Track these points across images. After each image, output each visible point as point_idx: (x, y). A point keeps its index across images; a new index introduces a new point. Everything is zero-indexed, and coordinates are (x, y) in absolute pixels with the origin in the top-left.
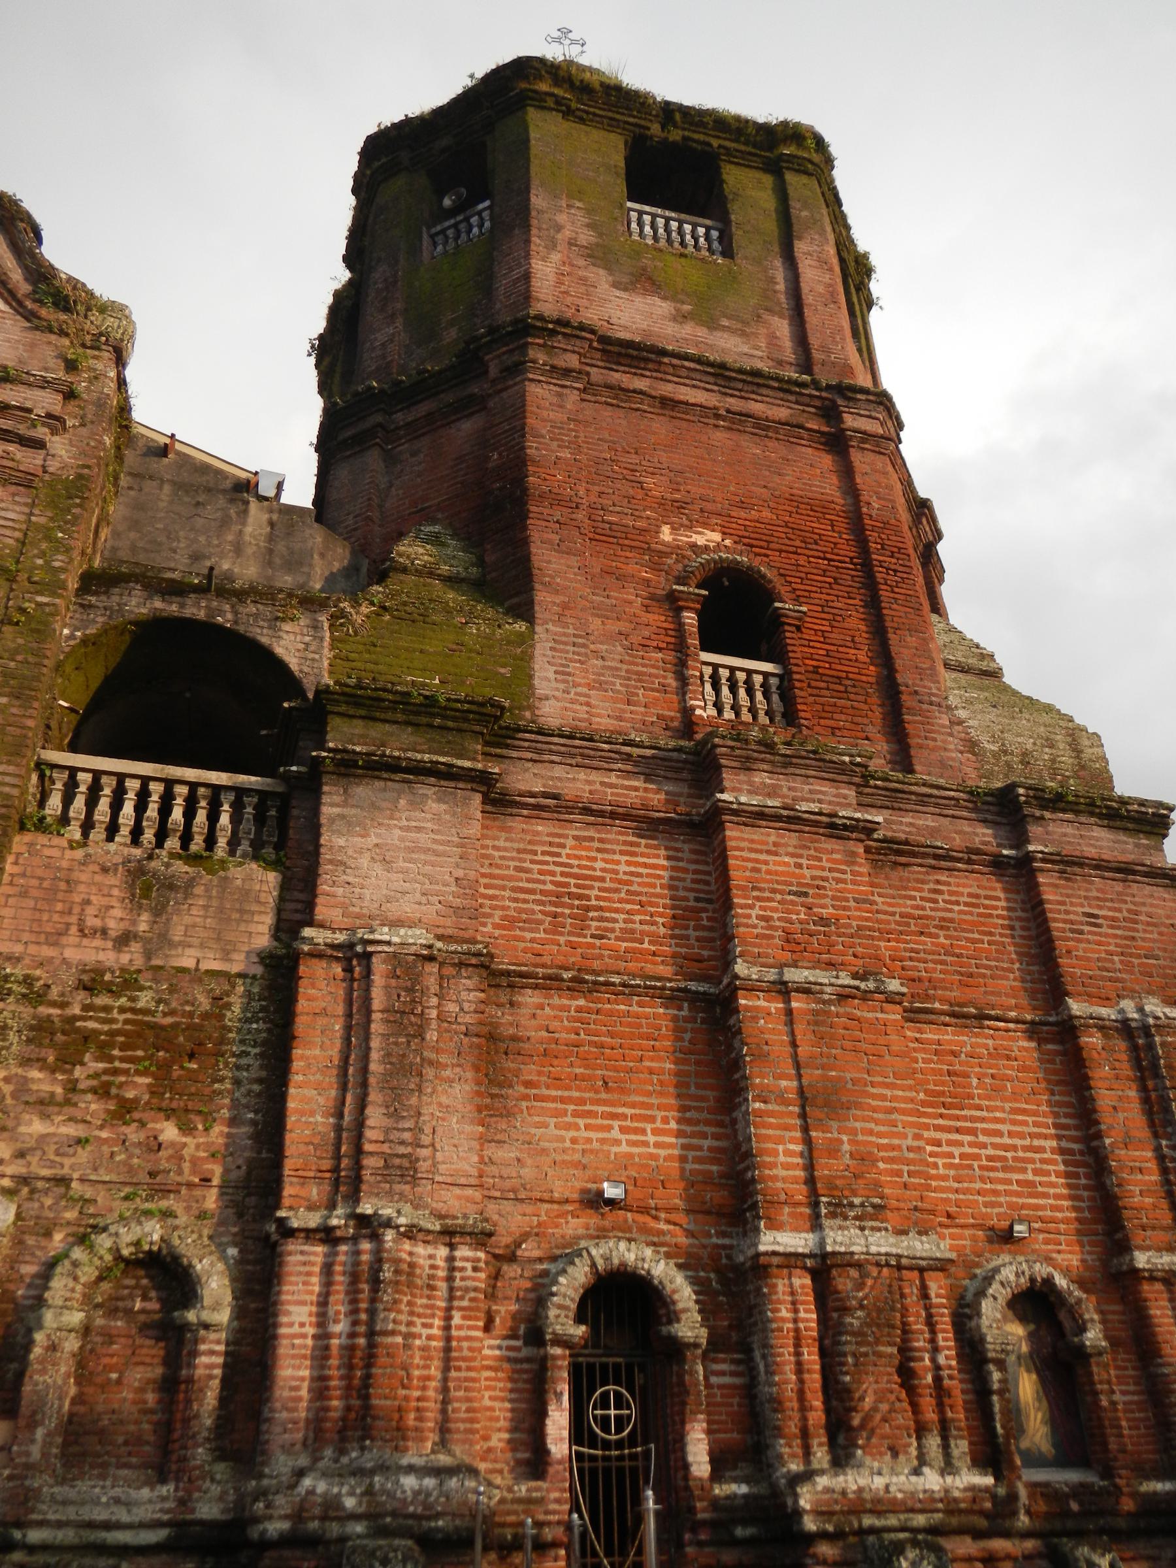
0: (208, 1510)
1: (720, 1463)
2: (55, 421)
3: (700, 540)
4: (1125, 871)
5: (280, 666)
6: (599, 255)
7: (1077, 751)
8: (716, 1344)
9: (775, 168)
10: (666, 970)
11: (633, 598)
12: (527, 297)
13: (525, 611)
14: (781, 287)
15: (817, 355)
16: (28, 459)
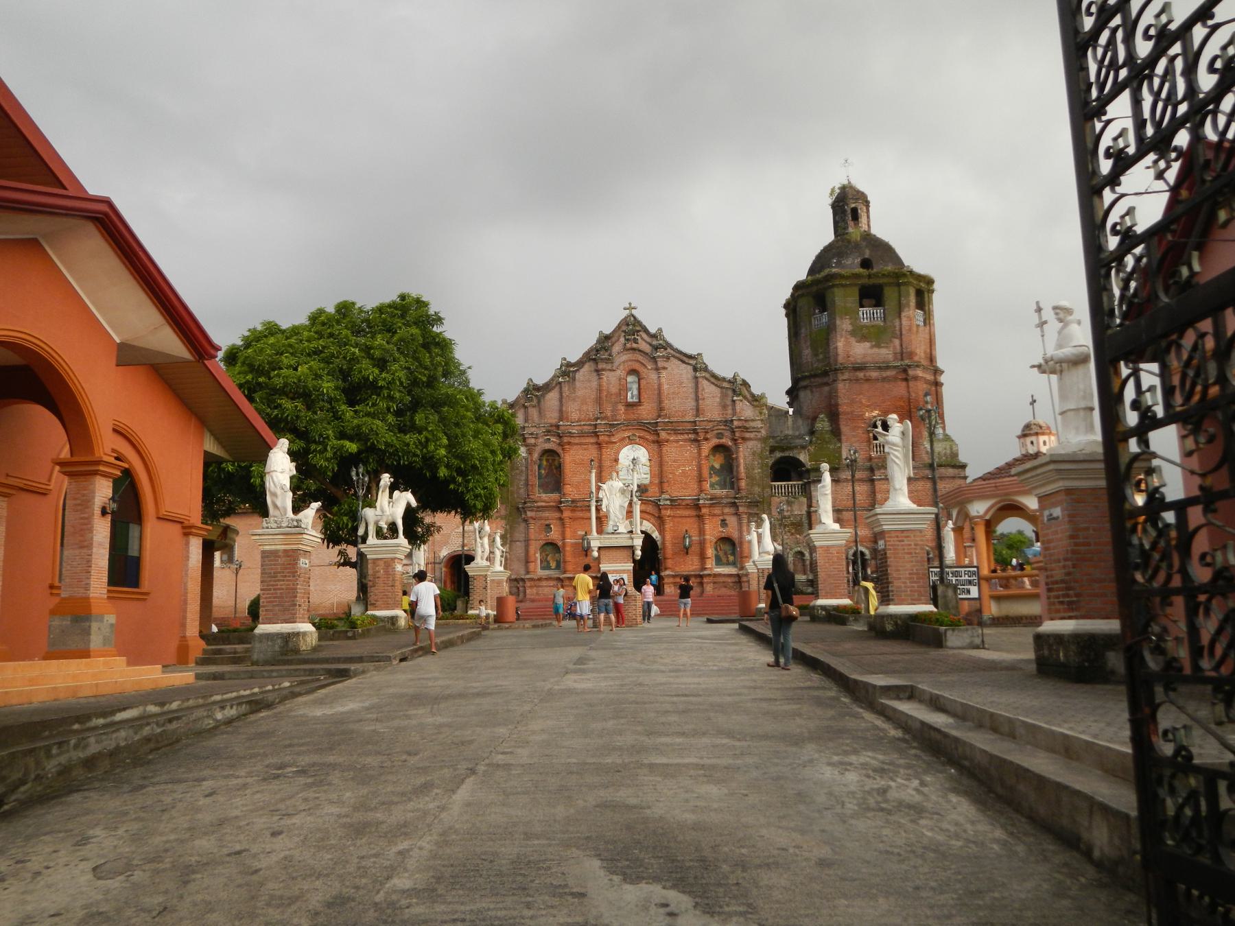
0: (810, 578)
1: (872, 573)
2: (762, 427)
3: (874, 414)
4: (954, 478)
5: (801, 461)
6: (853, 333)
7: (951, 449)
8: (872, 558)
9: (899, 285)
10: (866, 505)
11: (860, 431)
12: (837, 354)
13: (840, 440)
14: (897, 328)
15: (904, 351)
16: (759, 435)
